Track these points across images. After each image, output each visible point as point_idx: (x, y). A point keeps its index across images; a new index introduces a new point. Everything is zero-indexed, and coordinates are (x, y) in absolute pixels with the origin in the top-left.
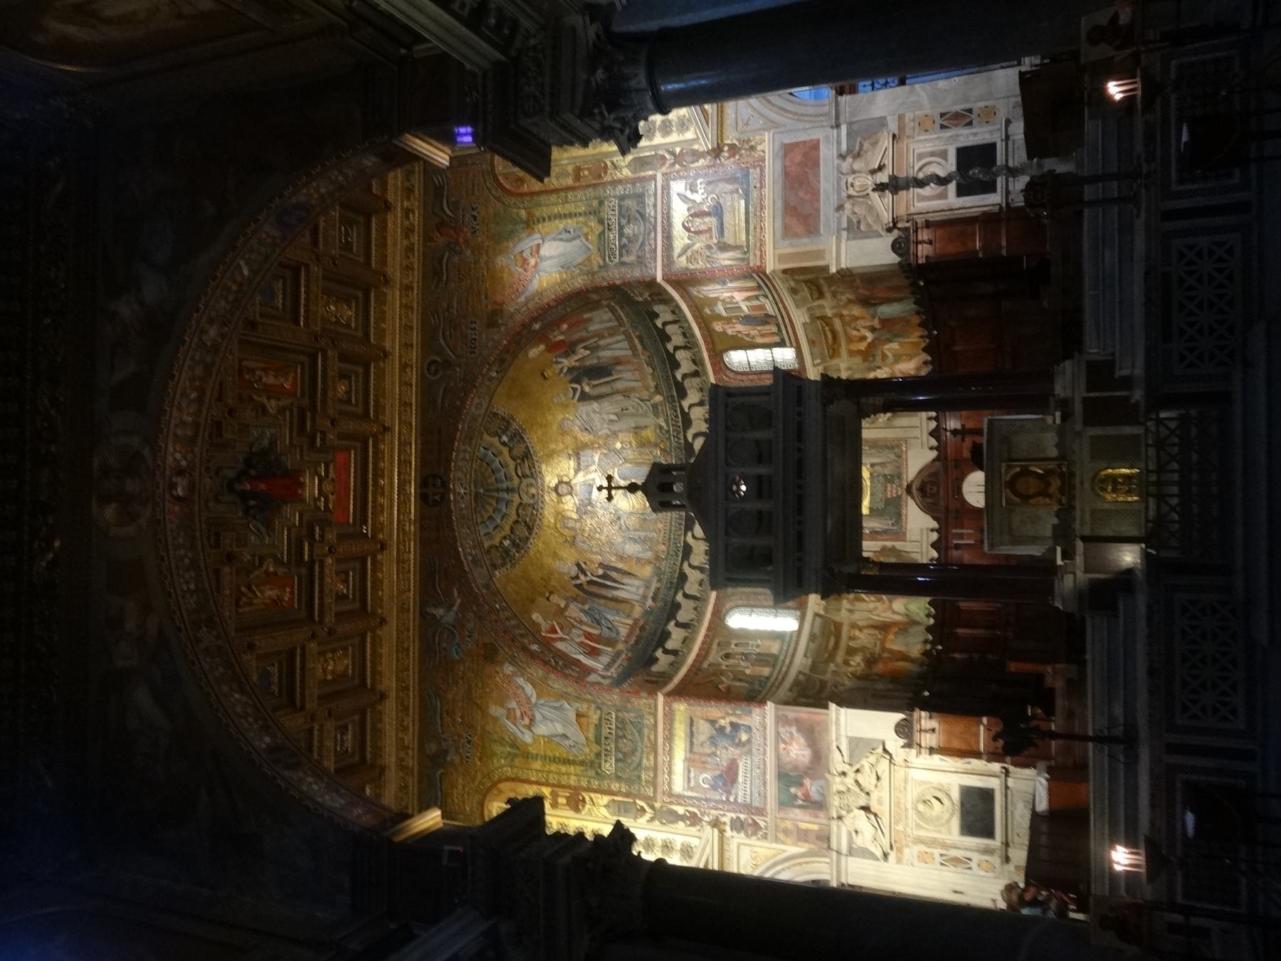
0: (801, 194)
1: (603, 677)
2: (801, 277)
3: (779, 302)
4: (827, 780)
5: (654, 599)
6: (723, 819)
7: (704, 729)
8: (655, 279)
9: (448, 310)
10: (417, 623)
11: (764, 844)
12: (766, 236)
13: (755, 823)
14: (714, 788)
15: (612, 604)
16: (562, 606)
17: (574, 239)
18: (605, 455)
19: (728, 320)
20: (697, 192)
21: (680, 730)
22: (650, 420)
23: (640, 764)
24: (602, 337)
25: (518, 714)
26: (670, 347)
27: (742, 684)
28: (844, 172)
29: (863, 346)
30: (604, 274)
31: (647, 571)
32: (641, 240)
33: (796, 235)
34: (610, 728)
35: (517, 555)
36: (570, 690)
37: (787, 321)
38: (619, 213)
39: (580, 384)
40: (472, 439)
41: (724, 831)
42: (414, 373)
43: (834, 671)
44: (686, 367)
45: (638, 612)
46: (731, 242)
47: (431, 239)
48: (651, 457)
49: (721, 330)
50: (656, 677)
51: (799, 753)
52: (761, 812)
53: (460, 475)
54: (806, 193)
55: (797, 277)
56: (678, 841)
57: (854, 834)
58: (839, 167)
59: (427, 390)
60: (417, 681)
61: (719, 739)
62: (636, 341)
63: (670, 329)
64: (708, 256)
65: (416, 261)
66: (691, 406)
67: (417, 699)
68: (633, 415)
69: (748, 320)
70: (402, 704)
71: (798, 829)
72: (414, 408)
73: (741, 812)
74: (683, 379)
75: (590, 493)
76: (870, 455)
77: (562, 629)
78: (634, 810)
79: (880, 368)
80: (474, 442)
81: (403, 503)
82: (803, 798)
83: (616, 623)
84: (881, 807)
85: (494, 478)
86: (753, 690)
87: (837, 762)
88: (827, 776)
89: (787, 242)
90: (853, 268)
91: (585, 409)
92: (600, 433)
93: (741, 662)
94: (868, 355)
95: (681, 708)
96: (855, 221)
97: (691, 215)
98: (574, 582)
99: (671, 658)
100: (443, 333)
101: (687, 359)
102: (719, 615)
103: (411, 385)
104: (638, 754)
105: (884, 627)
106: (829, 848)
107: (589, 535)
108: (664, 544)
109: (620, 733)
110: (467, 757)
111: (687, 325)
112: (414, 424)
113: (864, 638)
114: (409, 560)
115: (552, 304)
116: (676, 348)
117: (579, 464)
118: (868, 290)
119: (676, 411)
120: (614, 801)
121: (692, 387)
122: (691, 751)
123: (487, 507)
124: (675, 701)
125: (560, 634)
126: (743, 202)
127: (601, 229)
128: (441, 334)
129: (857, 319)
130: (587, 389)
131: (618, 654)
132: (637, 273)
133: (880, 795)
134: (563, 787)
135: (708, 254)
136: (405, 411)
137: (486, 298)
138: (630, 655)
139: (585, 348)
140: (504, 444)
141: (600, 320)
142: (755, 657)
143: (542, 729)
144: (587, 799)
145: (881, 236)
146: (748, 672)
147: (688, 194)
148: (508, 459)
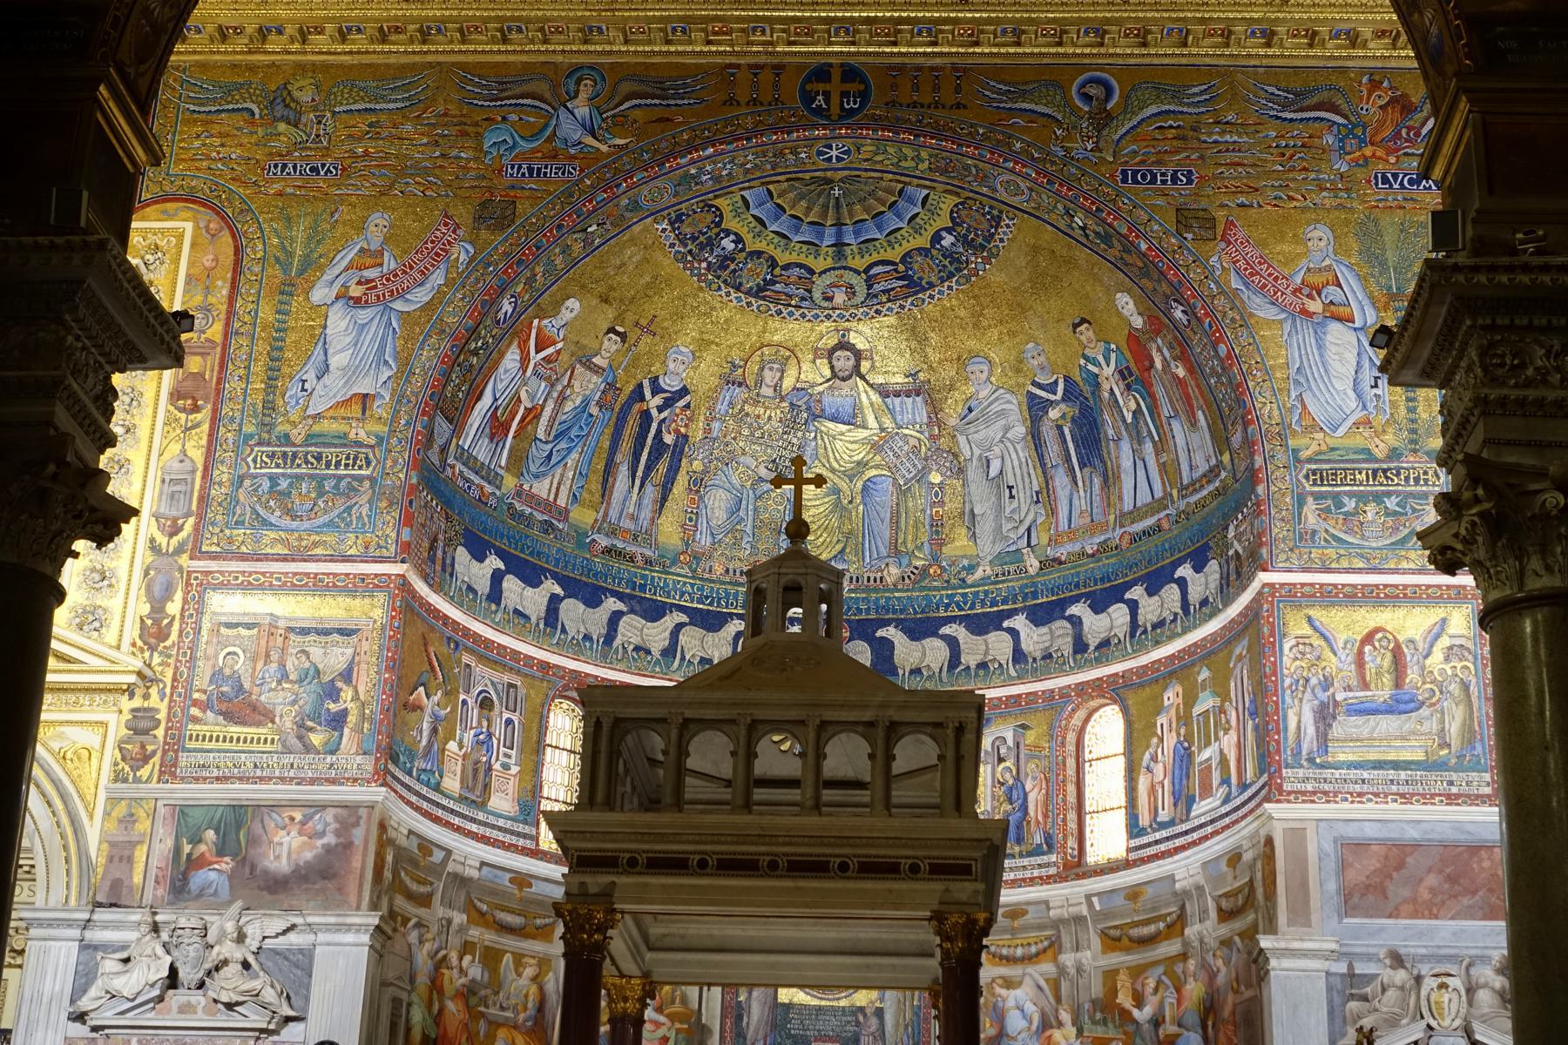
0: (1432, 880)
1: (444, 450)
2: (1259, 875)
4: (230, 903)
5: (608, 551)
6: (154, 691)
7: (334, 657)
8: (1265, 570)
9: (1219, 123)
10: (560, 58)
11: (104, 781)
12: (1346, 805)
13: (146, 759)
14: (217, 676)
15: (601, 466)
17: (1359, 396)
18: (915, 450)
20: (1447, 659)
21: (332, 609)
22: (987, 547)
23: (266, 524)
24: (1160, 448)
25: (370, 274)
26: (1136, 593)
27: (425, 734)
28: (1473, 971)
29: (1125, 1000)
30: (1281, 457)
32: (1350, 539)
33: (1343, 866)
34: (338, 464)
35: (704, 265)
36: (417, 381)
37: (1178, 842)
38: (1411, 494)
39: (1063, 400)
40: (944, 172)
41: (132, 696)
42: (1087, 51)
43: (449, 921)
44: (1096, 625)
45: (584, 517)
46: (1337, 730)
47: (1375, 85)
48: (910, 546)
49: (1166, 703)
50: (444, 559)
51: (285, 846)
52: (168, 771)
53: (869, 148)
54: (1431, 890)
55: (1259, 865)
56: (112, 603)
57: (124, 955)
58: (1485, 959)
59: (1051, 77)
60: (441, 58)
61: (313, 687)
62: (1150, 522)
63: (1171, 593)
64: (1307, 680)
65: (1333, 50)
66: (1014, 633)
67: (404, 60)
68: (1000, 508)
69: (1184, 757)
70: (398, 30)
71: (133, 845)
72: (1012, 50)
73: (167, 729)
74: (1071, 619)
75: (834, 419)
76: (900, 1010)
77: (547, 360)
78: (174, 513)
79: (1080, 1033)
80: (937, 176)
81: (806, 30)
82: (194, 857)
83: (559, 471)
84: (175, 1008)
85: (866, 217)
86: (412, 756)
87: (264, 926)
88: (239, 904)
89: (1329, 847)
90: (1269, 983)
91: (1013, 408)
92: (962, 439)
93: (472, 732)
96: (1368, 990)
97: (1398, 646)
98: (646, 383)
99: (483, 587)
100: (1168, 112)
101: (1111, 629)
103: (1060, 44)
104: (287, 522)
106: (100, 905)
107: (747, 415)
108: (727, 571)
109: (328, 485)
110: (285, 166)
111: (1179, 630)
112: (978, 50)
114: (690, 43)
115: (1222, 349)
117: (897, 394)
118: (1233, 1013)
119: (1005, 602)
120: (193, 472)
121: (1052, 639)
122: (290, 629)
123: (804, 203)
124: (393, 597)
125: (536, 358)
126: (1419, 756)
127: (1380, 453)
128: (1172, 108)
130: (1054, 414)
131: (494, 480)
132: (1278, 530)
133: (200, 1007)
134: (223, 365)
135: (1314, 681)
136: (1004, 32)
137: (1242, 205)
138: (492, 502)
139: (1137, 413)
140: (937, 238)
142: (484, 759)
143: (339, 322)
144: (199, 416)
146: (452, 746)
147: (1445, 642)
148: (906, 247)
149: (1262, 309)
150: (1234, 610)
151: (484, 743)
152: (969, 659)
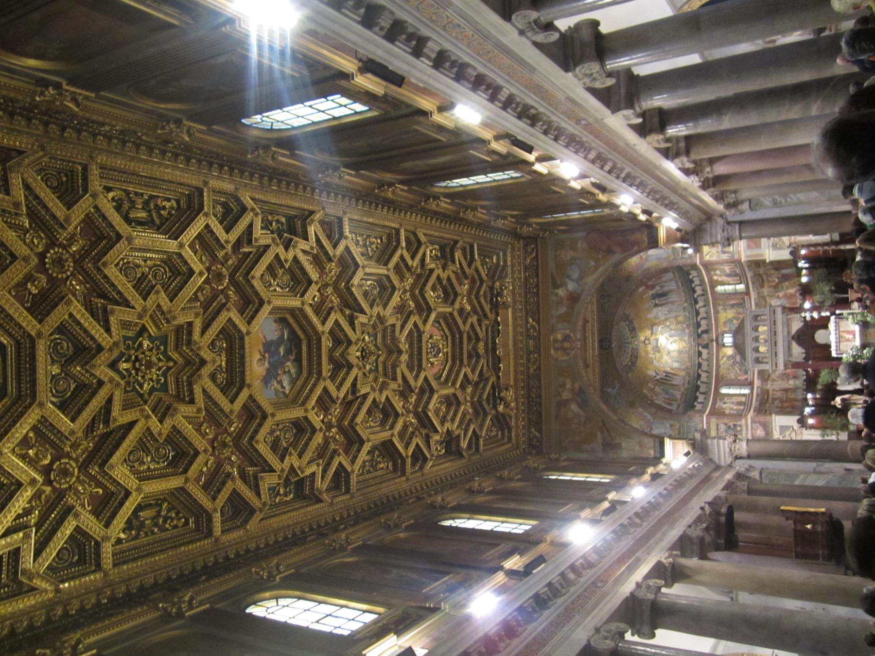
7: (722, 427)
8: (696, 264)
22: (682, 313)
24: (666, 282)
29: (774, 284)
45: (682, 389)
63: (694, 279)
69: (728, 275)
81: (593, 349)
91: (655, 310)
94: (776, 287)
95: (713, 420)
102: (717, 389)
105: (786, 390)
113: (779, 394)
129: (771, 275)
131: (679, 406)
132: (689, 261)
141: (669, 276)
145: (783, 249)
149: (646, 266)
150: (701, 267)
151: (733, 403)
152: (705, 315)
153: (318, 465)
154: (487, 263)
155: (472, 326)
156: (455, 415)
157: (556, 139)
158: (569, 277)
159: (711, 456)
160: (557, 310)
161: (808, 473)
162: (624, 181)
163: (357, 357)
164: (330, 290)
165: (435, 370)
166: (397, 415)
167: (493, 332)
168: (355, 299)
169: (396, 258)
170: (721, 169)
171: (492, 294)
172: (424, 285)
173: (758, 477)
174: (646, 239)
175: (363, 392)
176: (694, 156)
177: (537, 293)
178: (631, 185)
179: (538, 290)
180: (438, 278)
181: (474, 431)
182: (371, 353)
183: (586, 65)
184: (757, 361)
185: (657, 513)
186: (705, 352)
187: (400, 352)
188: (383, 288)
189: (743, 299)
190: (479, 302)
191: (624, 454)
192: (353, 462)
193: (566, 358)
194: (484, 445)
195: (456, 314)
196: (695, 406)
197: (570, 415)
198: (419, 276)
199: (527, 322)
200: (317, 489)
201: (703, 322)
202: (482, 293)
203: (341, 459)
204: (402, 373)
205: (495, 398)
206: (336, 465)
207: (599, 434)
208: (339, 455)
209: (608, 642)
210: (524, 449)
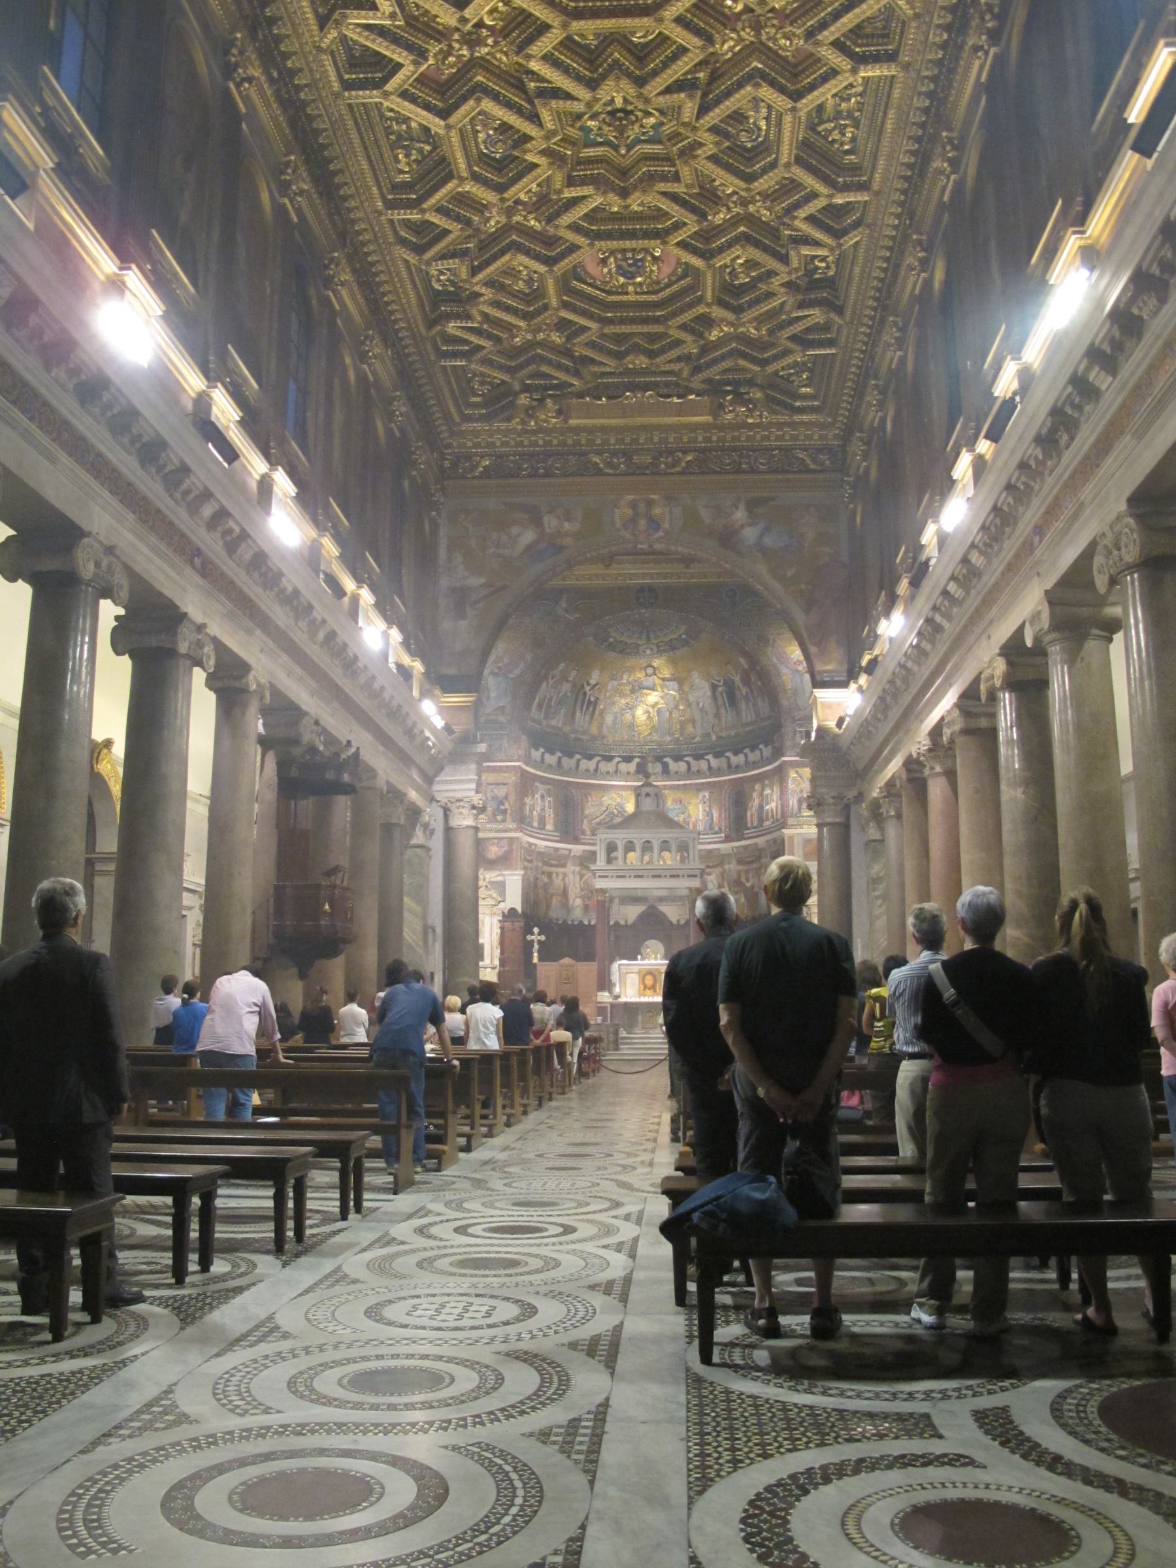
3: (769, 831)
7: (501, 792)
8: (783, 756)
16: (570, 679)
19: (761, 794)
22: (699, 731)
24: (755, 705)
26: (747, 751)
29: (743, 880)
31: (594, 730)
63: (757, 752)
66: (708, 761)
81: (636, 576)
91: (706, 686)
95: (512, 779)
99: (539, 759)
105: (565, 893)
113: (558, 881)
116: (746, 756)
125: (551, 682)
130: (720, 689)
132: (788, 743)
141: (764, 707)
149: (784, 670)
151: (543, 810)
152: (694, 768)
153: (393, 16)
154: (798, 374)
155: (678, 343)
156: (507, 309)
157: (1010, 487)
158: (767, 529)
159: (447, 769)
160: (705, 507)
161: (424, 917)
162: (929, 621)
163: (612, 101)
164: (748, 35)
165: (592, 268)
166: (501, 189)
167: (667, 384)
168: (728, 94)
169: (809, 181)
170: (937, 790)
171: (737, 383)
172: (757, 244)
173: (414, 841)
174: (829, 667)
175: (545, 116)
176: (960, 740)
177: (739, 471)
178: (919, 634)
179: (744, 472)
180: (771, 274)
181: (480, 348)
182: (621, 131)
183: (1135, 536)
184: (611, 848)
185: (340, 671)
186: (632, 767)
187: (624, 193)
188: (751, 155)
189: (720, 831)
190: (723, 358)
191: (446, 625)
192: (404, 95)
193: (618, 524)
194: (454, 366)
195: (701, 309)
196: (537, 749)
197: (515, 530)
198: (774, 233)
199: (685, 452)
200: (345, 17)
201: (682, 766)
202: (742, 362)
203: (408, 72)
204: (584, 197)
205: (544, 391)
206: (395, 57)
207: (483, 580)
208: (416, 63)
209: (91, 567)
210: (449, 446)
